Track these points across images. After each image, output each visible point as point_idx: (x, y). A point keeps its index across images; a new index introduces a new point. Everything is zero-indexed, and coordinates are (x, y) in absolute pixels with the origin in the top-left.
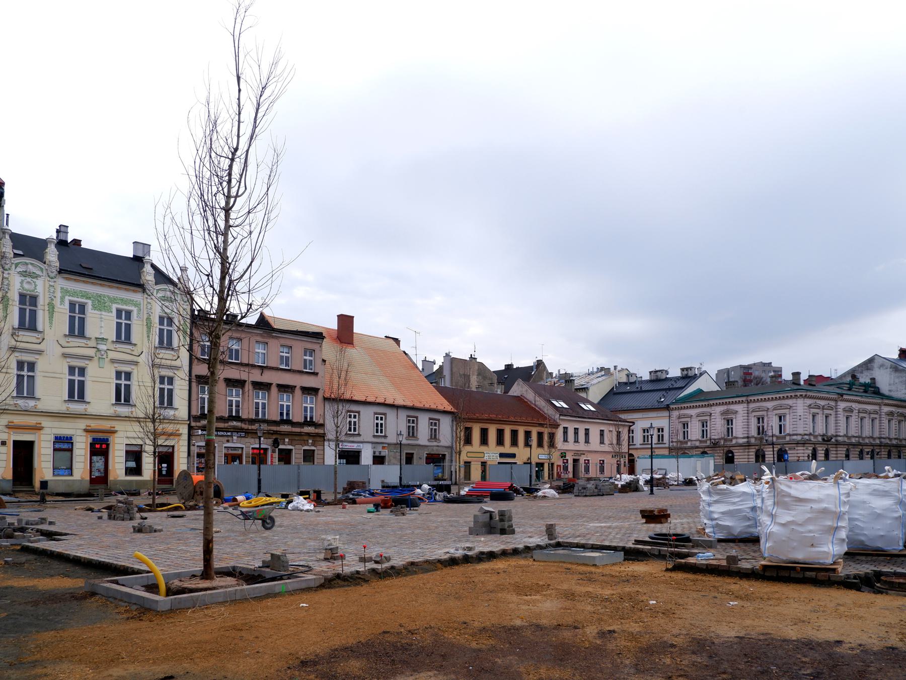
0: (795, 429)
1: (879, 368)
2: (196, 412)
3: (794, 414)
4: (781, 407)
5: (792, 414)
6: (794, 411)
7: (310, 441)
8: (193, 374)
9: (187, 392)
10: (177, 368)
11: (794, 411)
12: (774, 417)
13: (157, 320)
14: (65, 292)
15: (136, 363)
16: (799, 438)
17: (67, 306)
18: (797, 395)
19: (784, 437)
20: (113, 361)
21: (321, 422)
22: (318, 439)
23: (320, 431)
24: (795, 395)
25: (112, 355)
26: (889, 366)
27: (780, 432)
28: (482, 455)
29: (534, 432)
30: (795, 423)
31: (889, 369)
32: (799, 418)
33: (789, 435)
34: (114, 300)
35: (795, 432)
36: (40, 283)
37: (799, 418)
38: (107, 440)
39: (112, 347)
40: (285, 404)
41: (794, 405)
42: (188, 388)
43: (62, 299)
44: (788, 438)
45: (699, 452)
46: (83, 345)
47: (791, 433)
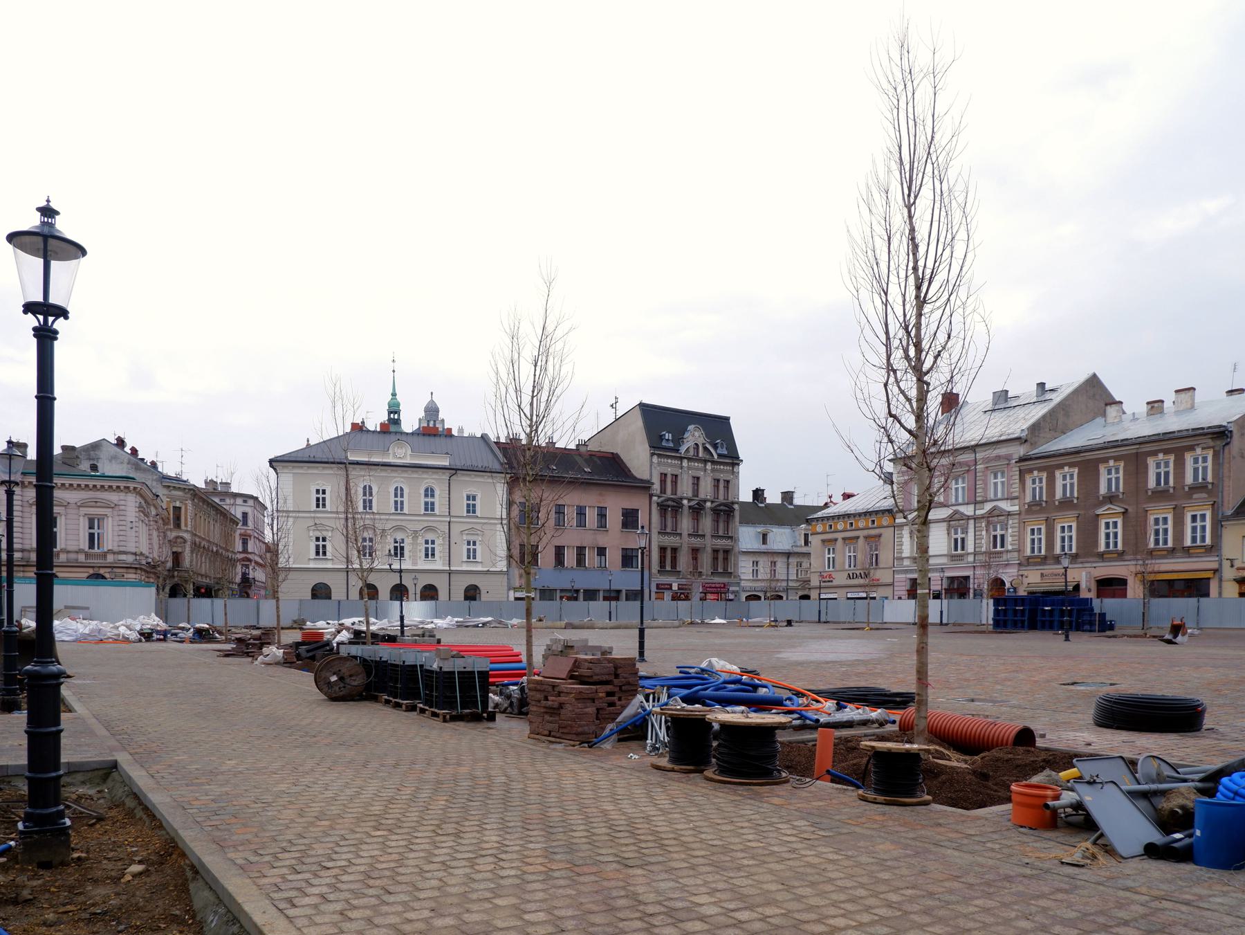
0: (122, 543)
1: (110, 461)
3: (122, 518)
4: (96, 503)
5: (117, 518)
6: (122, 513)
11: (122, 513)
12: (81, 518)
16: (130, 558)
18: (128, 488)
19: (104, 555)
24: (125, 487)
26: (126, 461)
27: (91, 546)
30: (122, 533)
31: (125, 465)
32: (130, 525)
33: (111, 552)
35: (122, 549)
37: (130, 525)
41: (122, 503)
44: (110, 558)
45: (86, 575)
47: (116, 549)
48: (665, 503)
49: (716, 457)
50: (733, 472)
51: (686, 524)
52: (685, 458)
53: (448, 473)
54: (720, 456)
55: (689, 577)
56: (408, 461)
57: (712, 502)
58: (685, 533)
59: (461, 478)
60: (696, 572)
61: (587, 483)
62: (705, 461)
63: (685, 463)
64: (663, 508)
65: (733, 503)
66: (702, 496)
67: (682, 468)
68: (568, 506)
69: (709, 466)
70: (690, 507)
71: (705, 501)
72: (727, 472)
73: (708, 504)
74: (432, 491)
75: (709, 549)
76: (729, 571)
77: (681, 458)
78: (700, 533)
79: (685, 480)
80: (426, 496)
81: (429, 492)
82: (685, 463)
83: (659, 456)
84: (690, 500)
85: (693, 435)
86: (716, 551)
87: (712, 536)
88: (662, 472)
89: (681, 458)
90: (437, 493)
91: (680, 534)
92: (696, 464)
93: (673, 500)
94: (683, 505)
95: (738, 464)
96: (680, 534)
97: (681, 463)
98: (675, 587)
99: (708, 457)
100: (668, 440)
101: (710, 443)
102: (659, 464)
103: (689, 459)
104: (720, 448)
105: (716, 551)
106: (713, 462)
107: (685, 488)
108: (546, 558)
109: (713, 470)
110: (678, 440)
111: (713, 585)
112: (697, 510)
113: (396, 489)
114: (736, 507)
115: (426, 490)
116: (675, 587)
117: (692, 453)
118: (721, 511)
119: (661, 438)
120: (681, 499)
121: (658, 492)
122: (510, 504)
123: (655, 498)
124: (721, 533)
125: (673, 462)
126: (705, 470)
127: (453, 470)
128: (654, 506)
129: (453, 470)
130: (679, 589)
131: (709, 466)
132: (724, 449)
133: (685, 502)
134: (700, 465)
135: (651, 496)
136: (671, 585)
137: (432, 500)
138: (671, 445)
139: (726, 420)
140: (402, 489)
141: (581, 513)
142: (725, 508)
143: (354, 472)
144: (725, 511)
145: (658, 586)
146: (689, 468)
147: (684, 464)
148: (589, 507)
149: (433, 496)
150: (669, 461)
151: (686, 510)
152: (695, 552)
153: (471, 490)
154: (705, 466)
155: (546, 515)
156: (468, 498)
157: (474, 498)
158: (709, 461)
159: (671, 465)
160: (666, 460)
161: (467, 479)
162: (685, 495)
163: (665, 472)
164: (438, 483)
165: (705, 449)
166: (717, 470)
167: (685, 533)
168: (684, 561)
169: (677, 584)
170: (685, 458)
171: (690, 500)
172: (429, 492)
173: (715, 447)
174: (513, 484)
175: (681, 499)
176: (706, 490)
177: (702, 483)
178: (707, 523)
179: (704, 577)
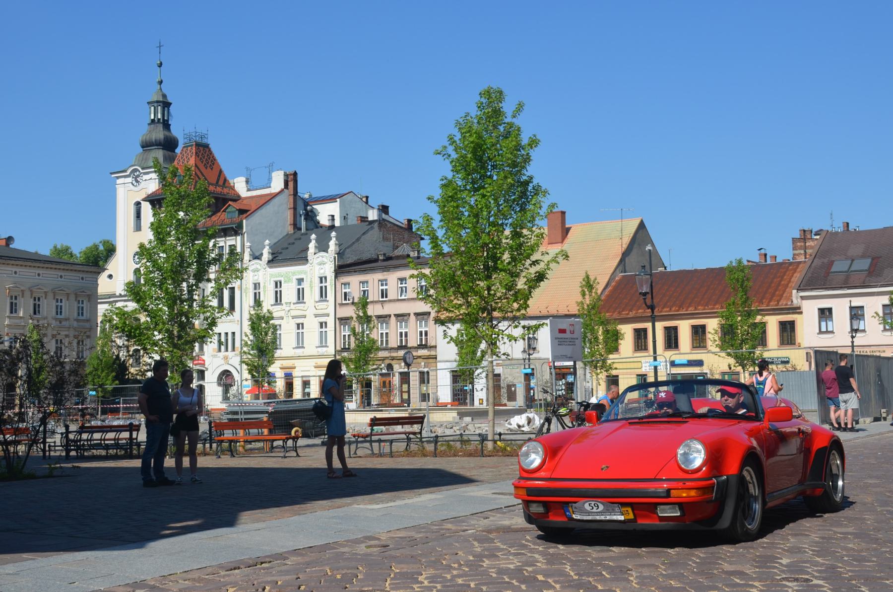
2: (338, 348)
7: (423, 364)
8: (337, 317)
9: (334, 332)
10: (328, 315)
13: (317, 280)
14: (271, 276)
15: (305, 317)
17: (273, 284)
20: (294, 317)
21: (433, 344)
22: (431, 360)
23: (433, 353)
25: (294, 313)
28: (639, 365)
29: (684, 328)
34: (294, 274)
36: (261, 273)
38: (291, 373)
39: (293, 306)
40: (384, 332)
42: (334, 329)
43: (270, 280)
46: (279, 309)
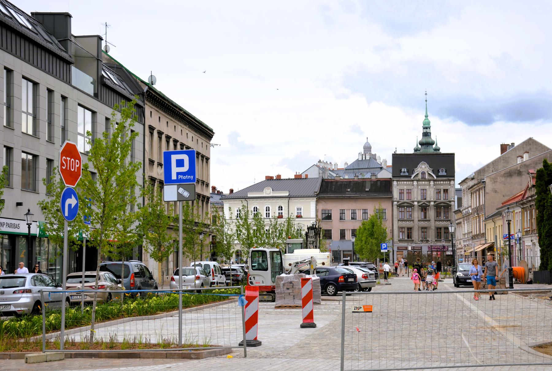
48: (402, 205)
49: (435, 178)
50: (450, 185)
51: (417, 214)
52: (414, 180)
53: (287, 199)
54: (437, 176)
55: (419, 243)
56: (271, 195)
57: (435, 202)
58: (416, 220)
59: (293, 201)
60: (425, 240)
61: (356, 198)
62: (429, 181)
63: (415, 183)
64: (399, 206)
65: (450, 202)
66: (428, 199)
67: (413, 185)
68: (347, 210)
69: (432, 183)
70: (419, 206)
71: (430, 202)
72: (446, 184)
73: (432, 203)
74: (282, 207)
75: (433, 228)
76: (449, 239)
77: (413, 181)
78: (427, 219)
79: (415, 193)
80: (279, 210)
81: (281, 208)
82: (415, 183)
83: (397, 181)
84: (418, 202)
85: (421, 167)
86: (438, 229)
87: (435, 220)
88: (407, 188)
89: (413, 181)
90: (283, 208)
91: (413, 220)
92: (423, 183)
93: (407, 203)
94: (414, 206)
95: (454, 180)
96: (413, 220)
97: (413, 183)
98: (410, 248)
99: (430, 178)
100: (404, 172)
101: (433, 172)
102: (398, 185)
103: (418, 181)
104: (441, 172)
105: (438, 229)
106: (434, 181)
107: (415, 196)
108: (336, 235)
109: (434, 185)
110: (411, 172)
111: (436, 247)
112: (424, 208)
113: (267, 208)
114: (452, 203)
115: (279, 207)
116: (410, 248)
117: (420, 177)
118: (442, 206)
119: (401, 172)
120: (413, 202)
121: (398, 199)
122: (317, 211)
123: (395, 203)
124: (442, 219)
125: (408, 183)
126: (430, 185)
127: (289, 197)
128: (395, 208)
129: (289, 197)
130: (412, 249)
131: (432, 183)
132: (444, 172)
133: (416, 203)
134: (426, 183)
135: (393, 202)
136: (406, 248)
137: (282, 212)
138: (407, 174)
139: (530, 139)
140: (269, 208)
141: (354, 213)
142: (444, 205)
143: (250, 201)
144: (443, 206)
145: (398, 248)
146: (418, 185)
147: (414, 184)
148: (358, 210)
149: (282, 210)
150: (405, 183)
151: (416, 208)
152: (424, 229)
153: (299, 206)
154: (430, 183)
155: (335, 216)
156: (298, 209)
157: (300, 209)
158: (431, 180)
159: (406, 185)
160: (403, 182)
161: (297, 201)
162: (416, 199)
163: (402, 188)
164: (283, 203)
165: (429, 174)
166: (438, 184)
167: (416, 220)
168: (416, 235)
169: (410, 247)
170: (414, 180)
171: (418, 202)
172: (281, 208)
173: (436, 172)
174: (317, 202)
175: (413, 202)
176: (431, 195)
177: (428, 193)
178: (431, 213)
179: (429, 243)
